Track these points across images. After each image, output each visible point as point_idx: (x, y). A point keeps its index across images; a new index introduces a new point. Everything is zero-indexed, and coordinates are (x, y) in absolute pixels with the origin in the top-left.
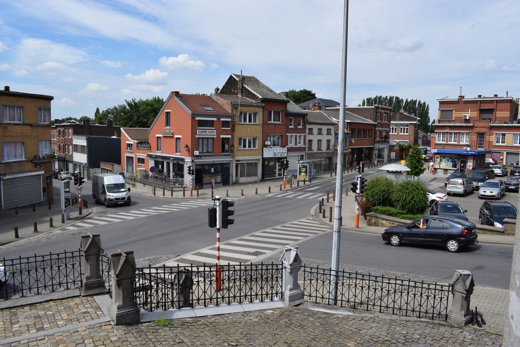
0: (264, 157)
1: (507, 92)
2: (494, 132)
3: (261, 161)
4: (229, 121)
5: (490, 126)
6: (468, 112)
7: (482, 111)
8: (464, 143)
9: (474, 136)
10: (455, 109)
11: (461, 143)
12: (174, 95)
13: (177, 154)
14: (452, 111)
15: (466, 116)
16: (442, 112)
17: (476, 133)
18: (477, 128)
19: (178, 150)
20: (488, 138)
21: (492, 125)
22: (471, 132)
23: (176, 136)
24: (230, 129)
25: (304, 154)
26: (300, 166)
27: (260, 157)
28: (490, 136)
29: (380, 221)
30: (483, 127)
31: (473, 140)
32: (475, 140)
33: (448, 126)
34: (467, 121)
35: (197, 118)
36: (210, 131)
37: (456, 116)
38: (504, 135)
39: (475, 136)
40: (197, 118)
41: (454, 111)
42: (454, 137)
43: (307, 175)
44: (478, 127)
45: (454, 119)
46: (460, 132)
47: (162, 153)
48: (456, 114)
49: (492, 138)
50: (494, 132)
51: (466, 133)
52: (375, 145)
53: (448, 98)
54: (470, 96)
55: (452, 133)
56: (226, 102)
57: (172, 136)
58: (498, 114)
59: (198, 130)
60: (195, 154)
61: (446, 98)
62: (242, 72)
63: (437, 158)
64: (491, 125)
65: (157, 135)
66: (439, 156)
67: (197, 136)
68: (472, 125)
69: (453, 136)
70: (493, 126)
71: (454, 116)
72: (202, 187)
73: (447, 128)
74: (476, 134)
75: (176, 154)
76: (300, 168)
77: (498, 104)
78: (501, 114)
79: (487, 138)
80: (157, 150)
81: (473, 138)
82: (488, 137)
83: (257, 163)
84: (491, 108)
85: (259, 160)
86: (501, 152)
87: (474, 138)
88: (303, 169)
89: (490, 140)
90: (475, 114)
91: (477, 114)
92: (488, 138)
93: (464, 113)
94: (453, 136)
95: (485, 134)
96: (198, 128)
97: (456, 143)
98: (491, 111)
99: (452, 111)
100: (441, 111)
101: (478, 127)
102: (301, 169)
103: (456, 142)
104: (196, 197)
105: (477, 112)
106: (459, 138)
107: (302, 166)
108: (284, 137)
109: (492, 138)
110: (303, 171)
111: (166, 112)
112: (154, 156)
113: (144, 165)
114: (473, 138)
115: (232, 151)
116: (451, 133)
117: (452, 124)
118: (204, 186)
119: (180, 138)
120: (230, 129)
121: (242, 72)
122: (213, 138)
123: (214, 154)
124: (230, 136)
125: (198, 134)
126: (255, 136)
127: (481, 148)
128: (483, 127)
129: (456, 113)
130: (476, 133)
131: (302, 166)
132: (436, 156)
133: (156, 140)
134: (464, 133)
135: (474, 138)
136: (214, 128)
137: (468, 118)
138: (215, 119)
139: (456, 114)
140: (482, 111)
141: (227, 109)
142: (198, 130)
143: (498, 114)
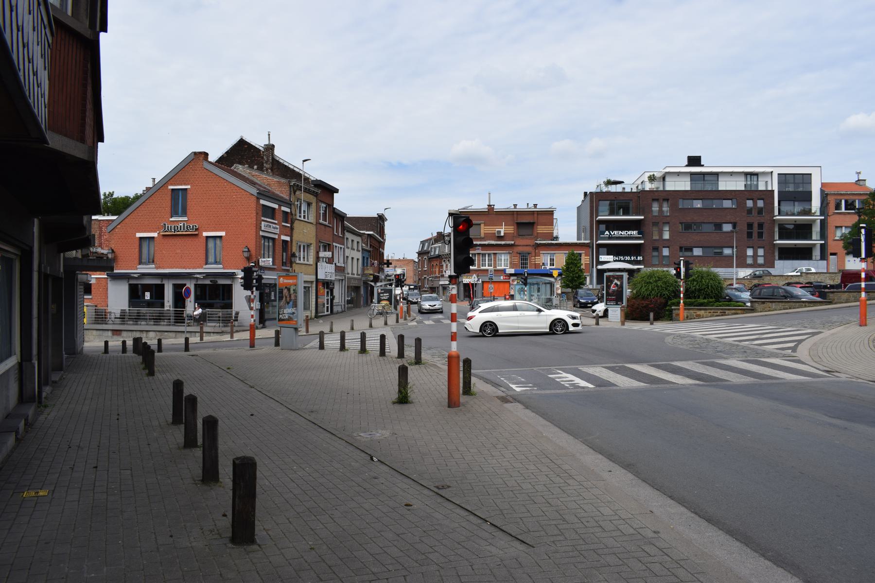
0: (318, 278)
1: (528, 204)
3: (314, 285)
4: (288, 212)
6: (501, 227)
12: (201, 158)
13: (207, 266)
14: (480, 224)
18: (519, 247)
19: (211, 259)
20: (534, 260)
21: (538, 242)
22: (511, 252)
23: (205, 234)
24: (289, 225)
25: (344, 278)
26: (380, 291)
27: (313, 278)
28: (536, 258)
29: (696, 313)
30: (527, 246)
31: (515, 263)
32: (517, 263)
33: (480, 245)
34: (500, 238)
35: (262, 202)
36: (274, 226)
37: (485, 232)
39: (517, 258)
40: (262, 202)
41: (482, 225)
42: (488, 259)
43: (391, 304)
45: (482, 235)
47: (157, 268)
48: (485, 230)
49: (539, 260)
52: (380, 273)
53: (473, 207)
54: (502, 204)
55: (485, 254)
56: (275, 180)
57: (197, 233)
58: (540, 229)
59: (263, 223)
60: (261, 264)
61: (470, 208)
62: (269, 135)
63: (513, 281)
64: (537, 242)
65: (139, 235)
66: (515, 278)
67: (261, 233)
68: (513, 242)
69: (487, 258)
70: (540, 244)
71: (482, 231)
72: (264, 325)
75: (204, 267)
76: (379, 294)
77: (540, 216)
78: (544, 229)
79: (532, 260)
80: (140, 264)
81: (514, 260)
82: (534, 258)
83: (309, 287)
84: (532, 221)
85: (312, 282)
87: (516, 260)
88: (385, 294)
89: (536, 262)
90: (511, 229)
91: (512, 229)
92: (534, 260)
94: (487, 258)
96: (263, 218)
98: (531, 225)
99: (480, 224)
102: (381, 295)
103: (491, 266)
104: (305, 334)
105: (513, 227)
107: (381, 290)
108: (332, 246)
109: (539, 260)
110: (384, 298)
111: (173, 190)
112: (136, 276)
113: (90, 297)
114: (514, 260)
115: (291, 263)
116: (484, 255)
117: (486, 243)
118: (267, 323)
119: (221, 237)
120: (289, 225)
121: (269, 135)
122: (274, 239)
123: (275, 267)
124: (288, 239)
125: (263, 229)
126: (311, 242)
128: (527, 246)
129: (485, 227)
131: (381, 290)
132: (512, 278)
133: (138, 245)
135: (516, 260)
136: (276, 222)
137: (502, 234)
138: (276, 206)
139: (485, 230)
140: (519, 225)
141: (278, 193)
142: (263, 223)
143: (540, 229)
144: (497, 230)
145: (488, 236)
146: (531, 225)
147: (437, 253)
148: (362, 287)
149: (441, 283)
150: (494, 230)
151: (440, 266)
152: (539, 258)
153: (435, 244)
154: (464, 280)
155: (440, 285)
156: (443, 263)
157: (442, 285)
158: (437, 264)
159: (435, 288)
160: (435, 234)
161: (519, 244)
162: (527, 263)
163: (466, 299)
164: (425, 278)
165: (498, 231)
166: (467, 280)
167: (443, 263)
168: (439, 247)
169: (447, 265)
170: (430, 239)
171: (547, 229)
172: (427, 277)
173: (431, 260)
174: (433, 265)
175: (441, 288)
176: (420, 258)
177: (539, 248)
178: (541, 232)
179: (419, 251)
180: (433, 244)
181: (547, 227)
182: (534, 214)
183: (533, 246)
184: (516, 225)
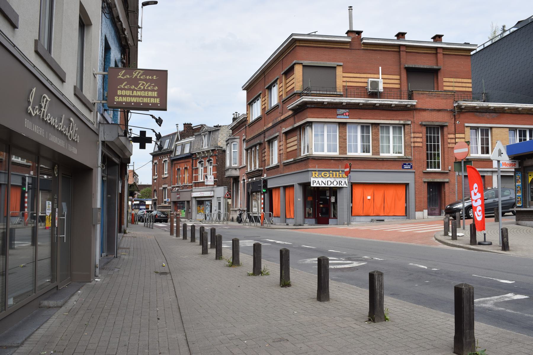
2: (466, 125)
5: (459, 107)
6: (376, 76)
7: (411, 71)
8: (391, 154)
9: (417, 135)
10: (342, 64)
11: (383, 155)
14: (335, 68)
15: (375, 84)
16: (308, 70)
17: (422, 125)
18: (424, 114)
20: (453, 141)
21: (463, 104)
22: (409, 122)
28: (458, 135)
30: (439, 110)
31: (416, 145)
32: (420, 145)
38: (485, 132)
39: (421, 135)
41: (339, 70)
42: (363, 137)
44: (424, 110)
46: (378, 124)
50: (466, 125)
51: (395, 126)
53: (317, 33)
58: (448, 84)
61: (314, 34)
70: (466, 107)
71: (340, 83)
73: (342, 111)
74: (424, 130)
79: (449, 141)
81: (416, 140)
82: (452, 136)
84: (435, 67)
86: (485, 174)
87: (419, 140)
92: (453, 141)
93: (369, 76)
95: (445, 129)
97: (369, 155)
98: (433, 73)
99: (335, 68)
100: (304, 66)
101: (424, 110)
103: (369, 152)
106: (376, 140)
114: (416, 140)
127: (435, 168)
128: (439, 110)
130: (422, 125)
134: (387, 126)
135: (419, 140)
143: (448, 84)
144: (370, 79)
145: (348, 91)
146: (433, 73)
147: (187, 151)
148: (100, 169)
149: (194, 195)
150: (366, 80)
151: (193, 169)
152: (462, 136)
153: (181, 139)
154: (312, 179)
155: (192, 198)
156: (198, 165)
157: (195, 198)
158: (186, 168)
159: (183, 202)
160: (181, 128)
161: (424, 107)
162: (438, 145)
163: (307, 220)
164: (165, 188)
165: (372, 82)
166: (320, 180)
167: (198, 165)
168: (191, 142)
169: (206, 168)
170: (175, 134)
171: (460, 85)
172: (168, 188)
173: (175, 162)
174: (179, 169)
175: (194, 202)
176: (156, 161)
177: (462, 116)
178: (451, 89)
179: (154, 152)
180: (177, 140)
181: (460, 80)
182: (436, 54)
183: (452, 111)
184: (404, 73)
